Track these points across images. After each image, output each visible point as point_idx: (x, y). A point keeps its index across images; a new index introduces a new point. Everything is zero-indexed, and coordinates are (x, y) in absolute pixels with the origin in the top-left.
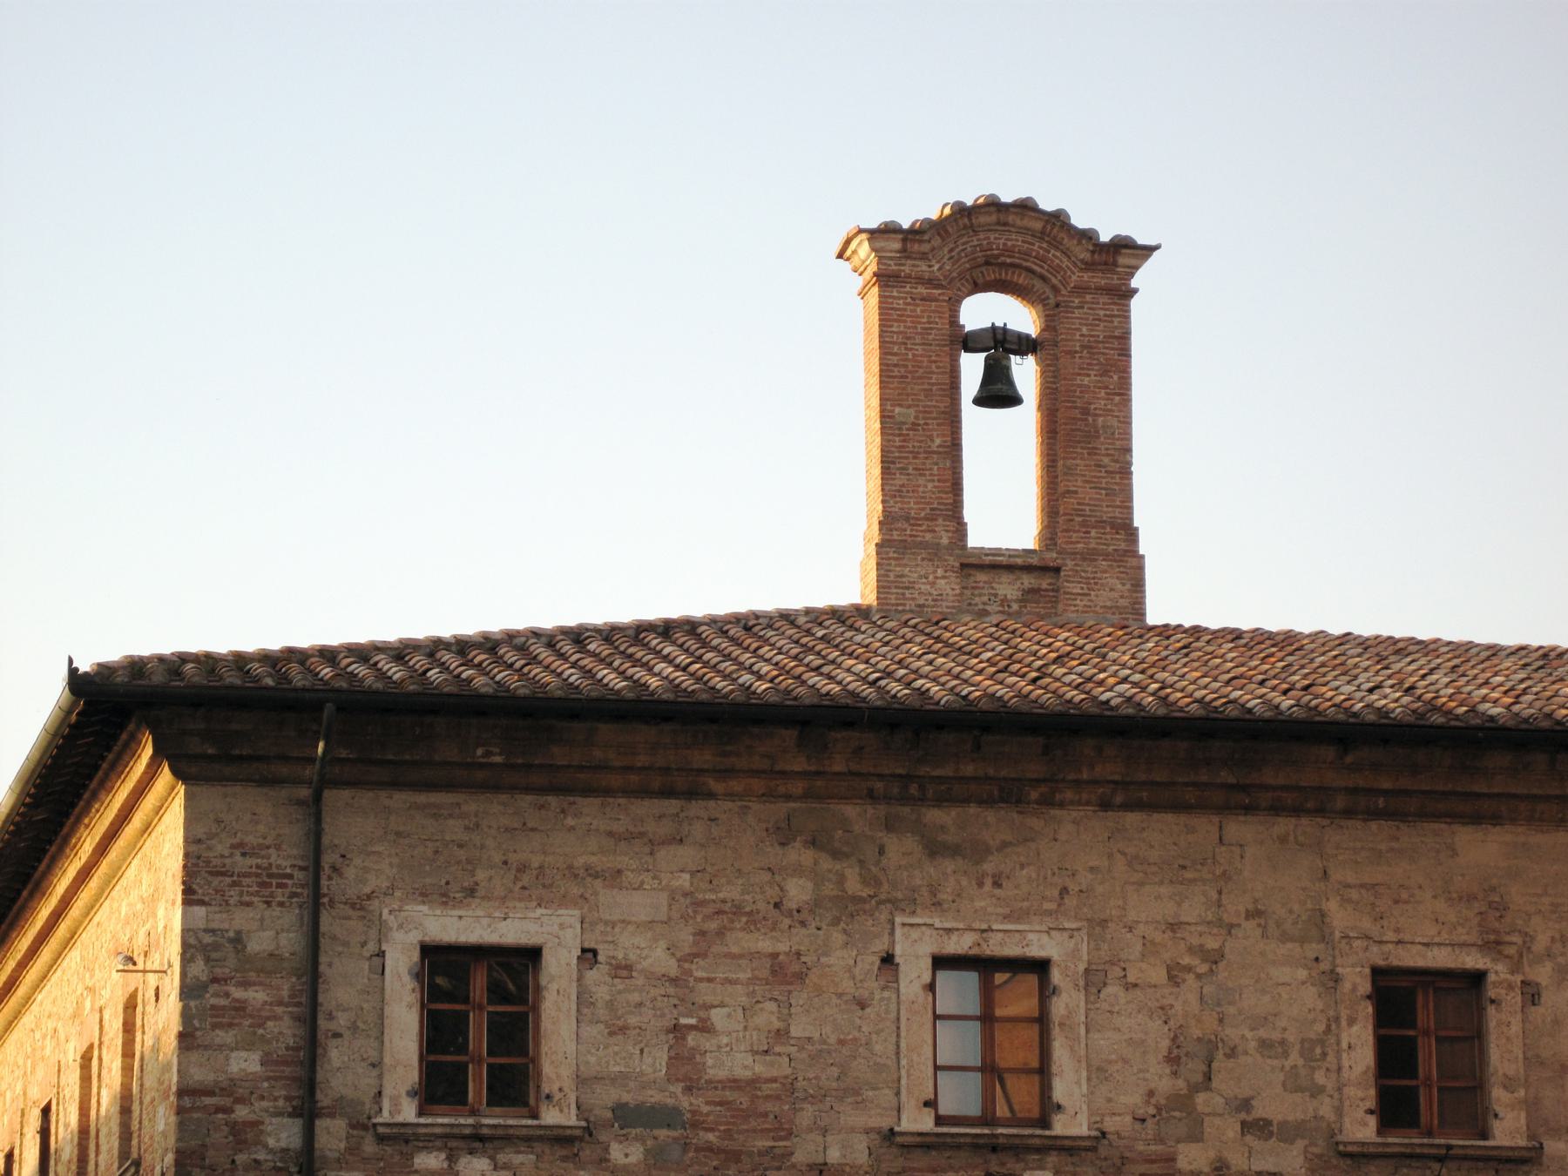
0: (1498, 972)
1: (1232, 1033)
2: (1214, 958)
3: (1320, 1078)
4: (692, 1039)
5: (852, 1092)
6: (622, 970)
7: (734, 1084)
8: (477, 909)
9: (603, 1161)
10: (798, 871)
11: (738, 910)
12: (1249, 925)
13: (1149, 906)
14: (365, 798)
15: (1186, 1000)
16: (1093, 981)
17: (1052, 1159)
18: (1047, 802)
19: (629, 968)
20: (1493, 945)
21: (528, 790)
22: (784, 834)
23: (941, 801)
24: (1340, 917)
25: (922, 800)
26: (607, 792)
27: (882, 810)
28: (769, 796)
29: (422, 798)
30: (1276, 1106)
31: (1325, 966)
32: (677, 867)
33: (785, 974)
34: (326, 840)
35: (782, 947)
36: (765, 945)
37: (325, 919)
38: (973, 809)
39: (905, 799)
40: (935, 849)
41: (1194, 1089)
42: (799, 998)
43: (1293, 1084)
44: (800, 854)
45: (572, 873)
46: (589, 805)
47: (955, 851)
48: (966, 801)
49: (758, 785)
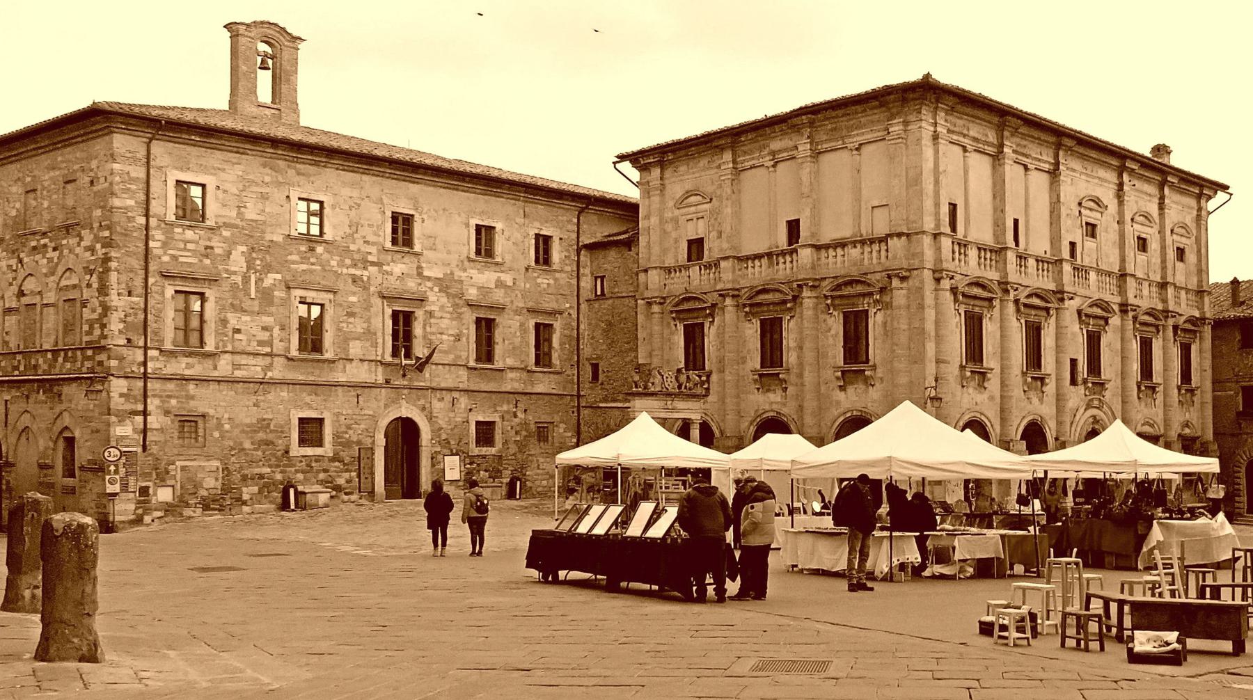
6: (225, 191)
15: (353, 213)
16: (333, 207)
22: (264, 166)
24: (385, 200)
30: (371, 238)
32: (238, 170)
33: (264, 197)
40: (299, 174)
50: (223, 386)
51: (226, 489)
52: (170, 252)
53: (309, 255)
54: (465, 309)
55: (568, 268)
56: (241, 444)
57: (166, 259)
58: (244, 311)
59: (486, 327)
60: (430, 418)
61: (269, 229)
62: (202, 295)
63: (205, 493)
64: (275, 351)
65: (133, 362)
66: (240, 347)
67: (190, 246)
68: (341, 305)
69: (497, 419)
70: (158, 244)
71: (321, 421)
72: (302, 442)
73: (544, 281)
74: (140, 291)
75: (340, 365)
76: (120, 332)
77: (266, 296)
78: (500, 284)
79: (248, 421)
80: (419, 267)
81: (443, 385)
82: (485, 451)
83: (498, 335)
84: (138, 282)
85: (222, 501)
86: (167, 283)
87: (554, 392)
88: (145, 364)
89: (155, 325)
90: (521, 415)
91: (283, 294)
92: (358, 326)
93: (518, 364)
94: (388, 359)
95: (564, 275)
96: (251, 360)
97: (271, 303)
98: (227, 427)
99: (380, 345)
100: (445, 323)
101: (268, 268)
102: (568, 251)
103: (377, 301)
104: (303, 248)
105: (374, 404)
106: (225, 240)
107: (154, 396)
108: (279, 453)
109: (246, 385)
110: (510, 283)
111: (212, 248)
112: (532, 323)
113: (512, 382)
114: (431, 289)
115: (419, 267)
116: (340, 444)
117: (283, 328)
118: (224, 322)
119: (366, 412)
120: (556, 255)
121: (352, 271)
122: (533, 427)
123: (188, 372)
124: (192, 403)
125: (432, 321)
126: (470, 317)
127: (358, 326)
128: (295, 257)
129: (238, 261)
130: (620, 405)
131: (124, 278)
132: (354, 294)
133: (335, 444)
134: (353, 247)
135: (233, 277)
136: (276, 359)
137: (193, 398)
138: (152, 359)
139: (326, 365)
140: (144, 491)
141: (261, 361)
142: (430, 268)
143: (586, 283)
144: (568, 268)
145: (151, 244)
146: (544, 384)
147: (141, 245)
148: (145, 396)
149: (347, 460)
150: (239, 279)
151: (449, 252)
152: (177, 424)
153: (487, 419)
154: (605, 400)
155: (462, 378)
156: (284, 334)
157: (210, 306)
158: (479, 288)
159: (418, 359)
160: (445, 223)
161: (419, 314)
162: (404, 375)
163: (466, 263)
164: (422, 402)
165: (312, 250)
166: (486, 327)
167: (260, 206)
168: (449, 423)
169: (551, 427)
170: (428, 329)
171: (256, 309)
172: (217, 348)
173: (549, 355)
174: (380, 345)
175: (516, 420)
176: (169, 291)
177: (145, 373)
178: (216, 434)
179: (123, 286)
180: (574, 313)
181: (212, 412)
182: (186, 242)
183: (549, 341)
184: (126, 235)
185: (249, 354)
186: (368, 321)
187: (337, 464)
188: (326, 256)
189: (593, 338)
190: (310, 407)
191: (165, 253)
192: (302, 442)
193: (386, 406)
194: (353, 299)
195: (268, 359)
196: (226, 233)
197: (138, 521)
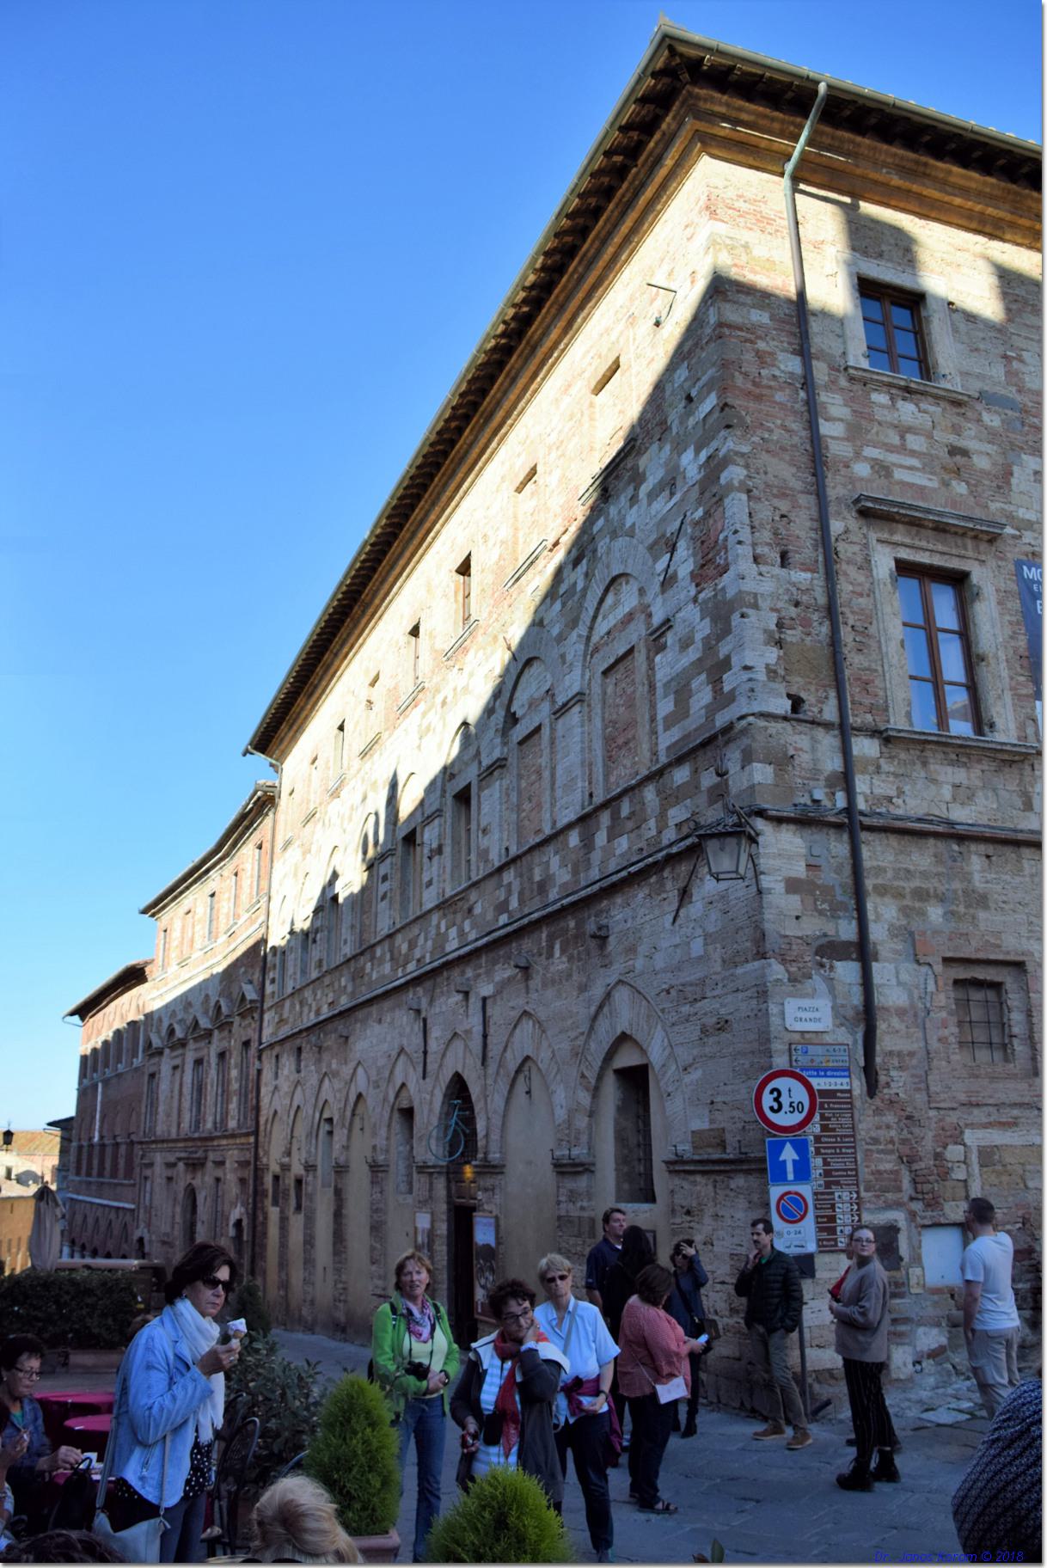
4: (1015, 364)
9: (979, 420)
52: (869, 452)
57: (862, 469)
62: (958, 580)
65: (815, 773)
67: (914, 442)
76: (771, 672)
84: (802, 528)
86: (873, 536)
88: (846, 779)
107: (882, 891)
111: (965, 453)
123: (962, 815)
131: (764, 512)
135: (1028, 537)
137: (982, 901)
145: (826, 428)
176: (884, 563)
177: (850, 810)
179: (766, 535)
182: (904, 431)
184: (759, 398)
191: (858, 455)
196: (992, 420)
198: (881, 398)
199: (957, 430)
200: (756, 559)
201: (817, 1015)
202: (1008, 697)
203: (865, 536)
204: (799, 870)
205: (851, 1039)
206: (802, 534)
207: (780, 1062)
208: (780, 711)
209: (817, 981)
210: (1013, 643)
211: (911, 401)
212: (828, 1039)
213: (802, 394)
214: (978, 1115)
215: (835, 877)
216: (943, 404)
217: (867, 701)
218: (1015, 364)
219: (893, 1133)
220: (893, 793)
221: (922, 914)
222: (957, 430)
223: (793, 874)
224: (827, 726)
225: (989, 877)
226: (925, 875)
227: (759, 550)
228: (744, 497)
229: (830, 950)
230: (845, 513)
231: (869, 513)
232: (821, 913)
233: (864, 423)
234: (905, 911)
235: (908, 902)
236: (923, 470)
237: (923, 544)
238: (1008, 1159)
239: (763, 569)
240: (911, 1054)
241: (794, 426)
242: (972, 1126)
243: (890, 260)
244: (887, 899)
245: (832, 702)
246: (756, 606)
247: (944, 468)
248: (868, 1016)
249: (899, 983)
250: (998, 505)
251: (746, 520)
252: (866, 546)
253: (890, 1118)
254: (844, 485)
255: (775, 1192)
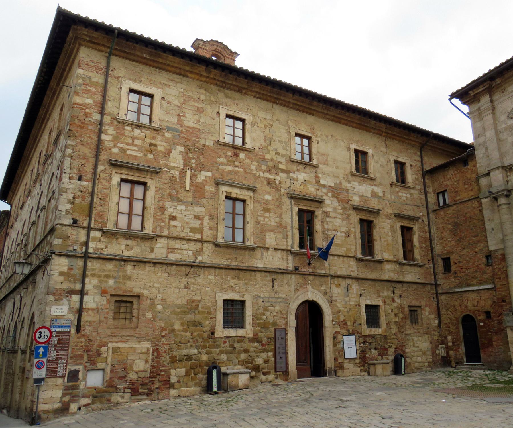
0: (313, 139)
1: (274, 138)
2: (272, 126)
3: (287, 148)
4: (182, 118)
5: (211, 133)
6: (169, 103)
7: (189, 127)
8: (141, 84)
9: (163, 136)
10: (203, 94)
11: (191, 98)
12: (277, 122)
13: (262, 114)
14: (120, 59)
15: (267, 131)
16: (253, 124)
17: (245, 152)
18: (246, 94)
19: (171, 102)
20: (313, 133)
21: (153, 66)
22: (201, 87)
23: (229, 89)
24: (291, 124)
25: (225, 88)
26: (168, 71)
27: (218, 88)
28: (198, 80)
29: (132, 62)
30: (280, 151)
31: (288, 130)
33: (200, 111)
34: (111, 64)
35: (199, 106)
36: (196, 105)
37: (109, 79)
38: (233, 92)
39: (222, 87)
40: (227, 96)
41: (268, 146)
42: (202, 115)
43: (283, 148)
44: (203, 91)
45: (160, 83)
46: (164, 73)
47: (230, 98)
48: (232, 90)
49: (197, 77)
50: (159, 268)
51: (156, 371)
52: (120, 145)
53: (234, 159)
54: (352, 212)
55: (418, 187)
56: (172, 325)
57: (115, 150)
58: (179, 201)
59: (367, 227)
60: (331, 302)
61: (202, 136)
62: (145, 184)
63: (134, 377)
64: (205, 238)
65: (76, 242)
66: (175, 232)
67: (137, 142)
68: (259, 202)
69: (381, 303)
70: (109, 138)
71: (243, 302)
72: (226, 324)
73: (404, 195)
74: (89, 176)
75: (258, 253)
76: (67, 212)
77: (198, 190)
78: (374, 194)
79: (178, 302)
80: (317, 177)
81: (339, 273)
82: (374, 331)
83: (376, 234)
84: (89, 168)
85: (150, 386)
86: (114, 171)
87: (418, 281)
89: (100, 208)
90: (397, 300)
91: (213, 189)
92: (272, 220)
93: (391, 258)
94: (296, 248)
95: (416, 192)
96: (184, 245)
97: (203, 196)
98: (159, 307)
99: (290, 237)
100: (338, 222)
101: (202, 167)
102: (416, 174)
103: (286, 201)
104: (229, 154)
105: (286, 288)
106: (167, 140)
107: (93, 275)
108: (206, 335)
109: (179, 268)
110: (381, 194)
111: (155, 146)
112: (398, 226)
113: (389, 272)
114: (326, 194)
115: (317, 177)
116: (259, 325)
117: (212, 218)
118: (162, 209)
119: (280, 295)
120: (410, 177)
121: (267, 175)
122: (407, 310)
123: (127, 254)
124: (129, 284)
125: (328, 219)
126: (355, 218)
127: (272, 220)
128: (222, 160)
129: (176, 159)
130: (476, 288)
131: (76, 164)
132: (269, 193)
133: (254, 325)
134: (268, 157)
135: (172, 171)
136: (205, 245)
137: (129, 278)
138: (95, 239)
139: (247, 252)
140: (73, 376)
141: (193, 247)
142: (325, 178)
143: (432, 198)
144: (418, 187)
145: (104, 137)
146: (411, 275)
147: (94, 137)
148: (84, 276)
149: (265, 340)
150: (177, 174)
151: (337, 167)
152: (113, 304)
153: (374, 303)
154: (458, 286)
155: (350, 268)
156: (212, 224)
157: (151, 194)
158: (361, 196)
159: (320, 249)
160: (335, 148)
161: (319, 213)
162: (309, 264)
163: (350, 177)
164: (323, 288)
165: (236, 155)
166: (367, 227)
167: (196, 117)
168: (345, 306)
169: (419, 310)
170: (326, 226)
171: (190, 200)
172: (155, 231)
173: (412, 251)
174: (290, 237)
175: (395, 304)
176: (116, 179)
177: (86, 253)
178: (149, 315)
179: (75, 171)
180: (425, 219)
181: (146, 292)
182: (134, 138)
183: (411, 241)
184: (82, 127)
185: (182, 239)
186: (280, 216)
187: (256, 344)
188: (247, 161)
189: (442, 238)
190: (234, 290)
191: (115, 146)
192: (226, 324)
193: (296, 290)
194: (268, 197)
195: (198, 245)
196: (168, 135)
197: (64, 410)
198: (129, 128)
199: (154, 138)
200: (70, 178)
201: (62, 311)
202: (152, 220)
203: (111, 171)
204: (65, 269)
205: (74, 317)
206: (88, 170)
207: (47, 324)
208: (68, 224)
209: (65, 301)
210: (158, 203)
211: (140, 129)
212: (65, 317)
213: (99, 126)
214: (114, 339)
215: (77, 272)
216: (151, 130)
217: (100, 220)
218: (182, 118)
219: (83, 344)
220: (103, 247)
221: (107, 282)
222: (154, 138)
223: (63, 271)
224: (84, 228)
225: (133, 271)
226: (110, 271)
227: (71, 175)
228: (69, 159)
229: (72, 292)
230: (106, 164)
231: (114, 165)
232: (70, 282)
233: (120, 136)
234: (101, 281)
235: (102, 278)
236: (138, 151)
237: (132, 174)
238: (123, 351)
239: (71, 181)
240: (94, 322)
241: (93, 137)
242: (111, 342)
243: (143, 83)
244: (95, 278)
245: (87, 221)
246: (66, 192)
247: (146, 150)
248: (80, 311)
249: (94, 301)
250: (163, 162)
251: (69, 166)
252: (111, 174)
253: (83, 339)
254: (107, 155)
255: (36, 360)
